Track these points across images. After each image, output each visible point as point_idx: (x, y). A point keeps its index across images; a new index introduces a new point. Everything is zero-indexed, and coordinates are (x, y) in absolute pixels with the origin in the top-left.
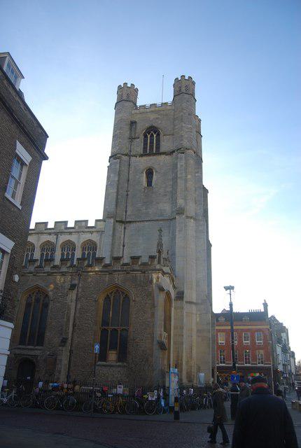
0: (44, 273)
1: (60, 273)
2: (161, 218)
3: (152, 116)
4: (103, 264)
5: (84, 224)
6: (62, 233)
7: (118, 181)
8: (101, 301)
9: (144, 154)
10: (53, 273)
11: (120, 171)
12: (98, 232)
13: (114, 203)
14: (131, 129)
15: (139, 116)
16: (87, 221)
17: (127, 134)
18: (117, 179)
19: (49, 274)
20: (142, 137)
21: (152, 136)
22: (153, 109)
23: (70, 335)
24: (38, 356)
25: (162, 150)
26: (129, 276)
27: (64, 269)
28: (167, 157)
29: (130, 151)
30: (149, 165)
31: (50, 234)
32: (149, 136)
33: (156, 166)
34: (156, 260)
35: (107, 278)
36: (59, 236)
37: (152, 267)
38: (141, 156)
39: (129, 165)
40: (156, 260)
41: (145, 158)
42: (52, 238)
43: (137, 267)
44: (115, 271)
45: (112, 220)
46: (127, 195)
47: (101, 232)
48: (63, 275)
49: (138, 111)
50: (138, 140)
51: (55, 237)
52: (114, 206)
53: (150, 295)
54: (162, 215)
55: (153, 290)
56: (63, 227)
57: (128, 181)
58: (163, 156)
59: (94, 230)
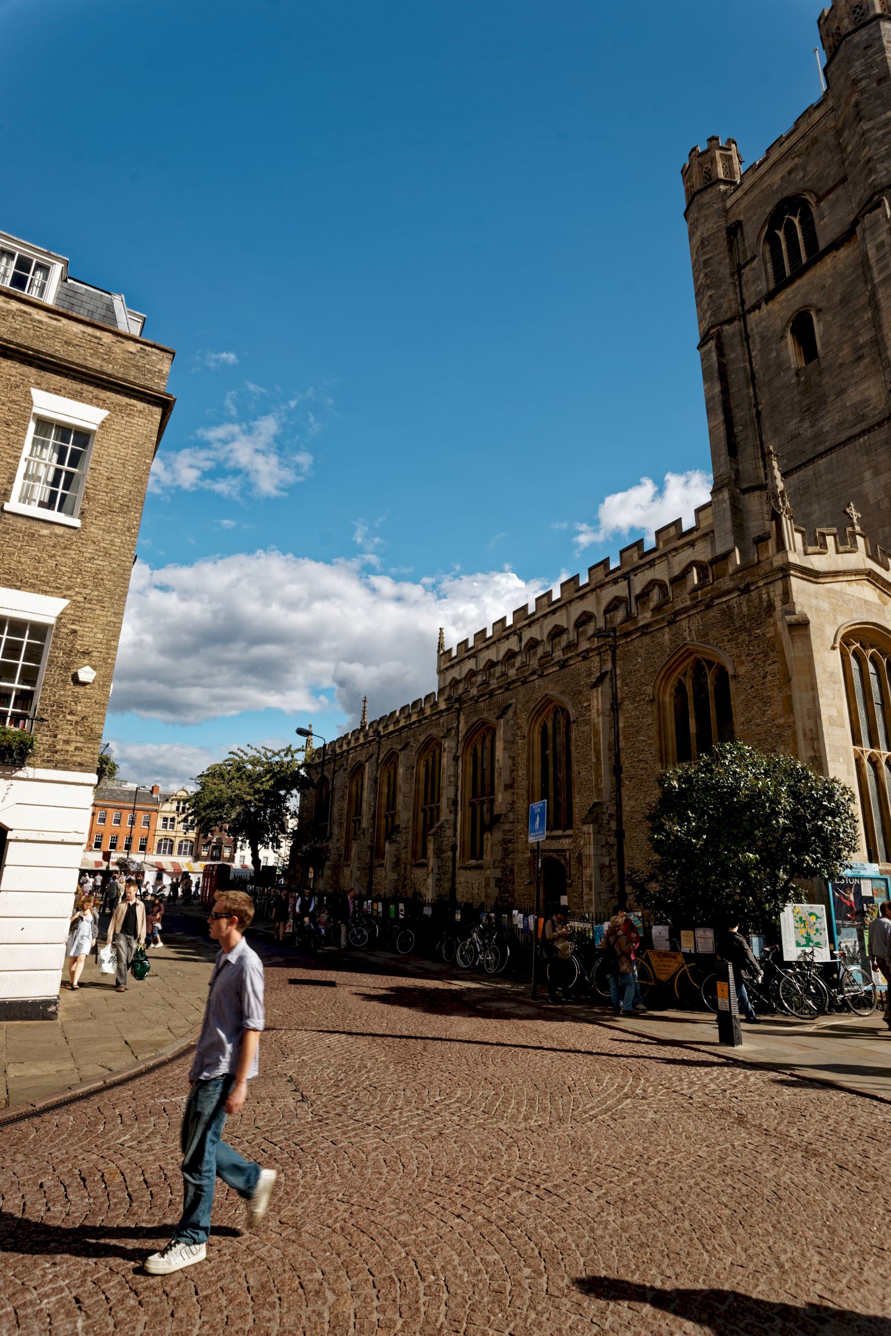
0: (553, 665)
1: (578, 655)
2: (863, 426)
3: (776, 178)
4: (652, 605)
5: (672, 531)
6: (636, 569)
7: (725, 391)
8: (668, 699)
9: (782, 283)
10: (567, 660)
11: (719, 368)
12: (707, 534)
13: (724, 449)
14: (730, 250)
15: (744, 203)
16: (678, 523)
17: (725, 270)
18: (717, 389)
19: (563, 665)
20: (764, 249)
21: (790, 226)
22: (775, 156)
23: (606, 796)
24: (564, 851)
25: (822, 245)
26: (713, 613)
27: (584, 645)
28: (842, 249)
29: (743, 302)
30: (797, 307)
31: (615, 581)
32: (781, 234)
33: (814, 299)
34: (772, 543)
35: (667, 637)
36: (632, 577)
37: (766, 567)
38: (770, 296)
39: (747, 337)
40: (772, 543)
41: (781, 297)
42: (620, 590)
43: (727, 583)
44: (677, 614)
45: (726, 494)
46: (759, 414)
47: (709, 535)
48: (584, 658)
49: (739, 193)
50: (755, 263)
51: (625, 583)
52: (724, 457)
53: (773, 647)
54: (862, 418)
55: (777, 634)
56: (636, 557)
57: (753, 376)
58: (828, 260)
59: (695, 535)
